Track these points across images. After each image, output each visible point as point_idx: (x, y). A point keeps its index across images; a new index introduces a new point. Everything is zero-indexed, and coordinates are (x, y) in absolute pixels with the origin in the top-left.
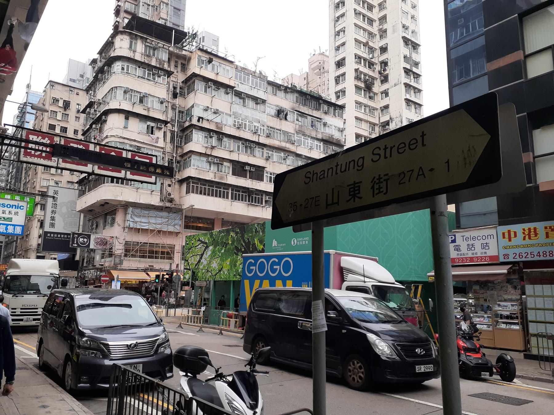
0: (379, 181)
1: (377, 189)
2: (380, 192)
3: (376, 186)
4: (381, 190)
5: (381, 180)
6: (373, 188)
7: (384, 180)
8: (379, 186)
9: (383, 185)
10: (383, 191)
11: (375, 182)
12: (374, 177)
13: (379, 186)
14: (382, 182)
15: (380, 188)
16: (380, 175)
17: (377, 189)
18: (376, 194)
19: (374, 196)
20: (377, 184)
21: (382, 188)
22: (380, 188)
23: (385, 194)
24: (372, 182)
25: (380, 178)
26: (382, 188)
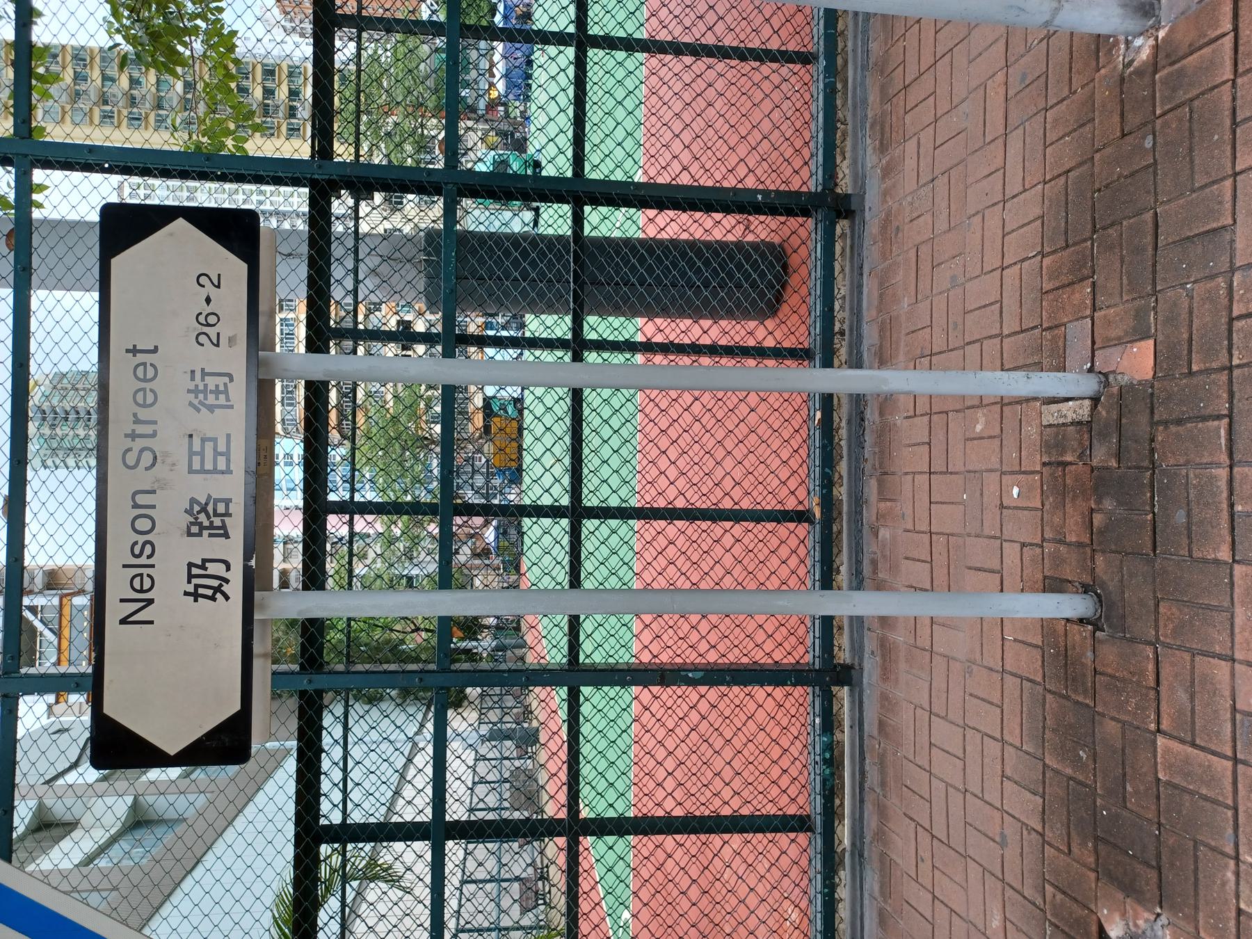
0: (201, 392)
1: (217, 399)
2: (226, 392)
3: (211, 399)
4: (222, 388)
5: (201, 387)
6: (211, 408)
7: (203, 380)
8: (211, 392)
9: (211, 382)
10: (225, 384)
11: (200, 402)
12: (191, 404)
13: (211, 392)
14: (206, 386)
15: (217, 392)
16: (189, 391)
17: (217, 399)
18: (228, 399)
19: (232, 407)
20: (206, 398)
21: (217, 386)
22: (217, 392)
23: (231, 380)
24: (198, 410)
25: (195, 391)
26: (217, 386)
